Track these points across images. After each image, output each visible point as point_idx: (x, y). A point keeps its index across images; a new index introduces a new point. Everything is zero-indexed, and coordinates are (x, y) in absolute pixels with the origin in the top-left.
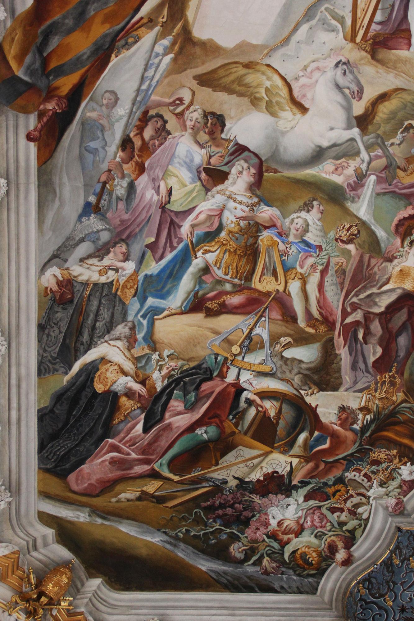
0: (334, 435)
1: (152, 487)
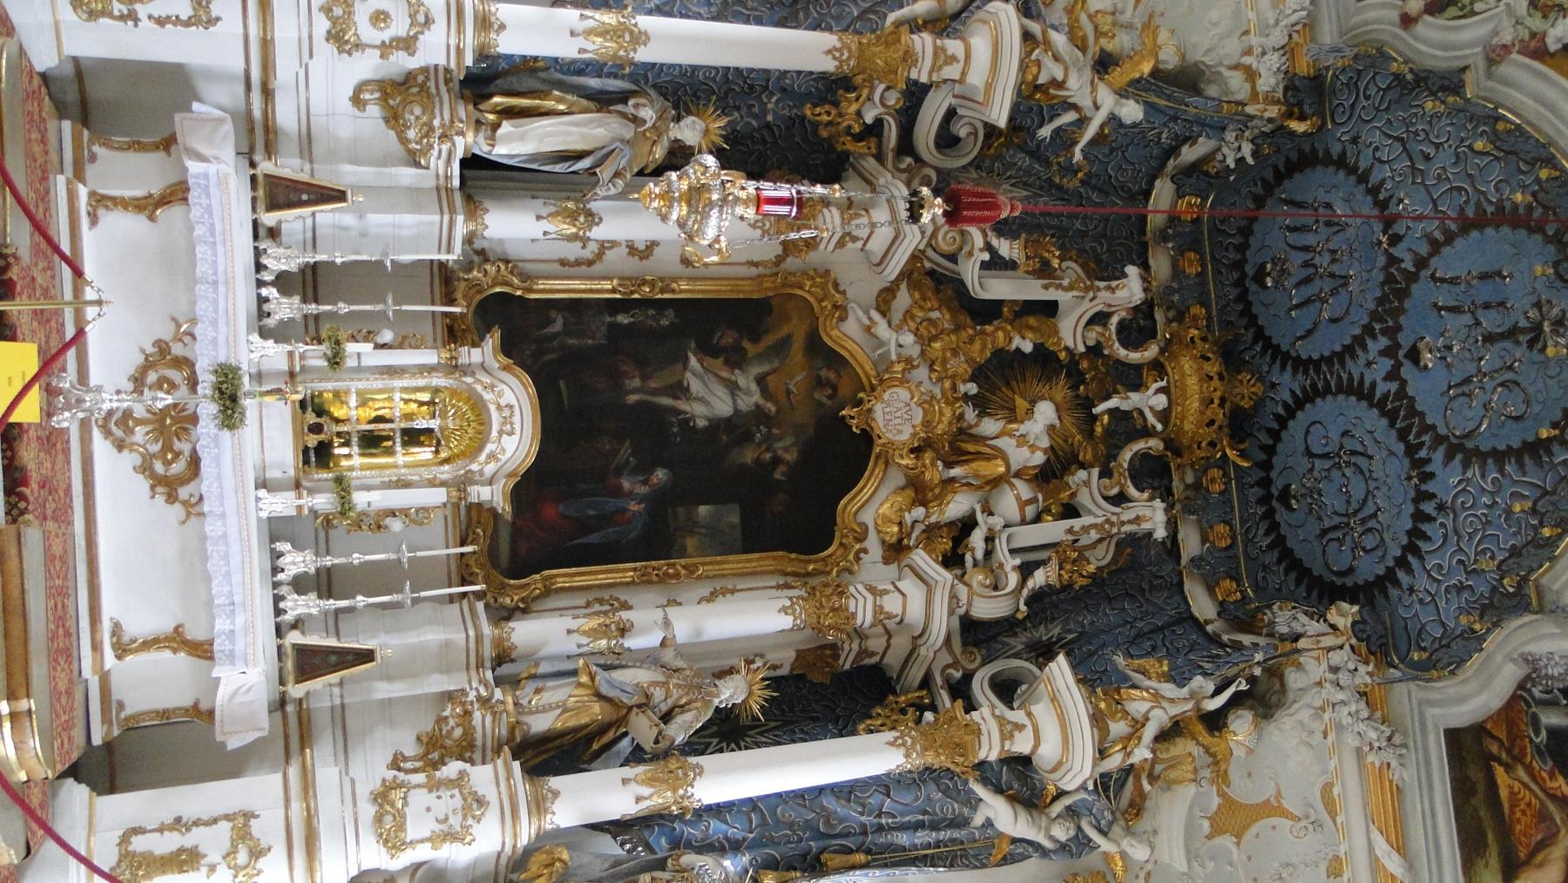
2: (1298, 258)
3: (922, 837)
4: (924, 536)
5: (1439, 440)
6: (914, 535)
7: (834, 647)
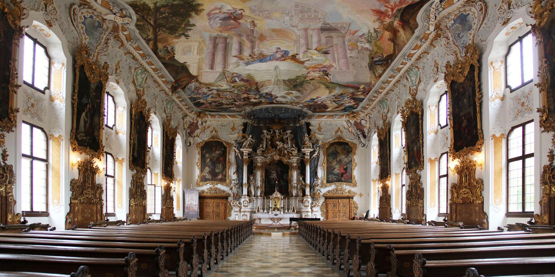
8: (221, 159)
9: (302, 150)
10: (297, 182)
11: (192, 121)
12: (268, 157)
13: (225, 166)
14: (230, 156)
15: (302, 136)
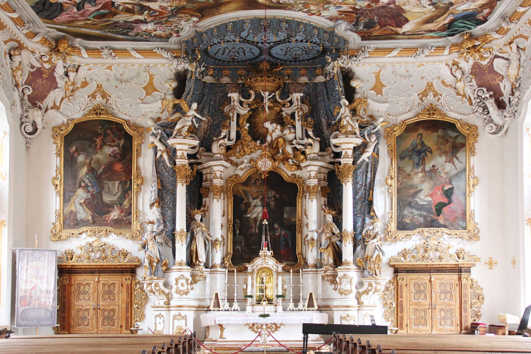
0: (159, 12)
1: (89, 22)
2: (231, 53)
3: (369, 175)
4: (296, 158)
5: (288, 38)
6: (296, 162)
7: (322, 188)
8: (118, 167)
9: (334, 141)
10: (319, 228)
11: (39, 66)
12: (243, 163)
13: (127, 186)
14: (141, 160)
15: (332, 108)
